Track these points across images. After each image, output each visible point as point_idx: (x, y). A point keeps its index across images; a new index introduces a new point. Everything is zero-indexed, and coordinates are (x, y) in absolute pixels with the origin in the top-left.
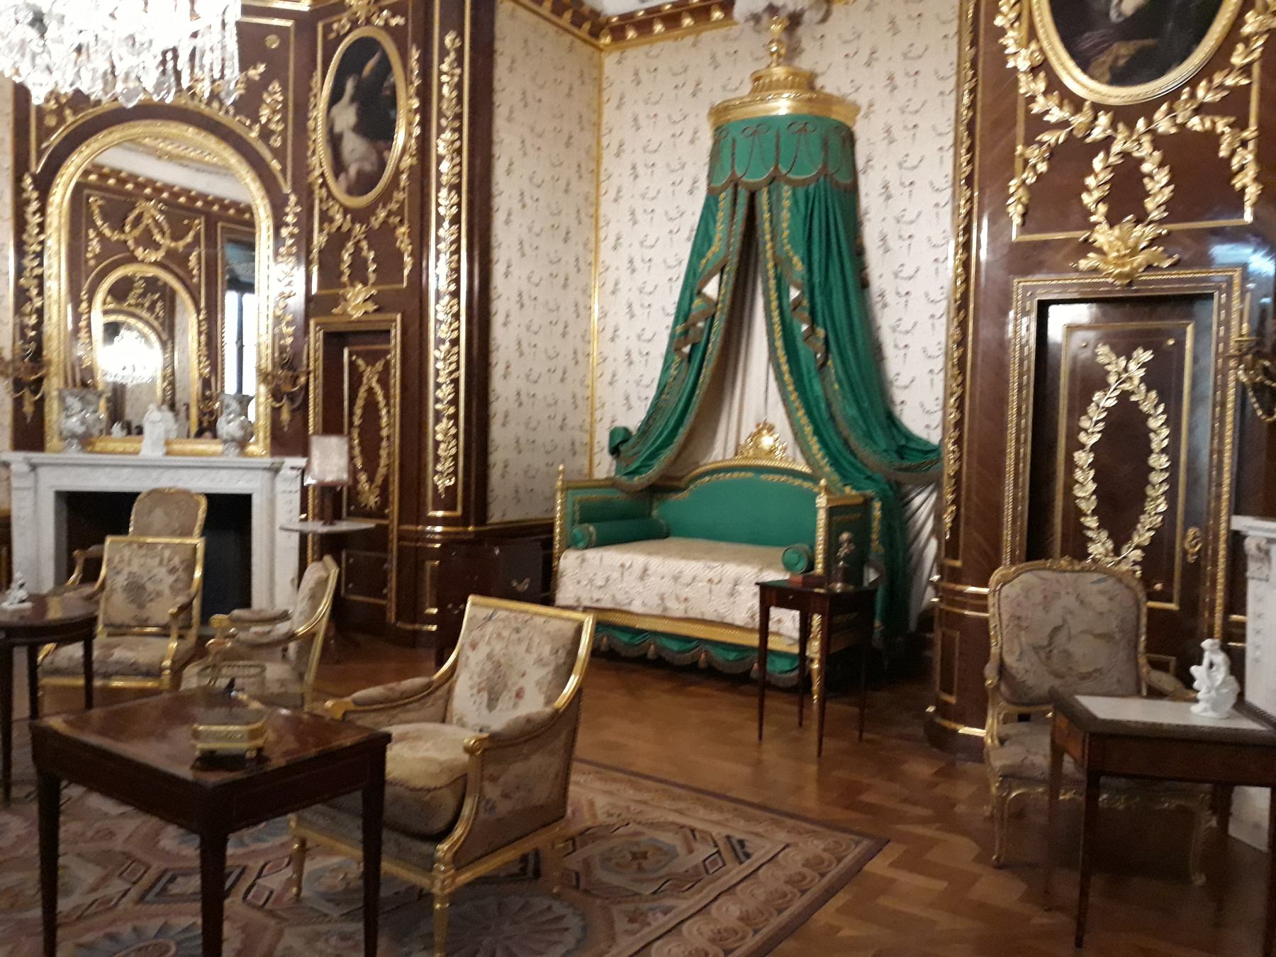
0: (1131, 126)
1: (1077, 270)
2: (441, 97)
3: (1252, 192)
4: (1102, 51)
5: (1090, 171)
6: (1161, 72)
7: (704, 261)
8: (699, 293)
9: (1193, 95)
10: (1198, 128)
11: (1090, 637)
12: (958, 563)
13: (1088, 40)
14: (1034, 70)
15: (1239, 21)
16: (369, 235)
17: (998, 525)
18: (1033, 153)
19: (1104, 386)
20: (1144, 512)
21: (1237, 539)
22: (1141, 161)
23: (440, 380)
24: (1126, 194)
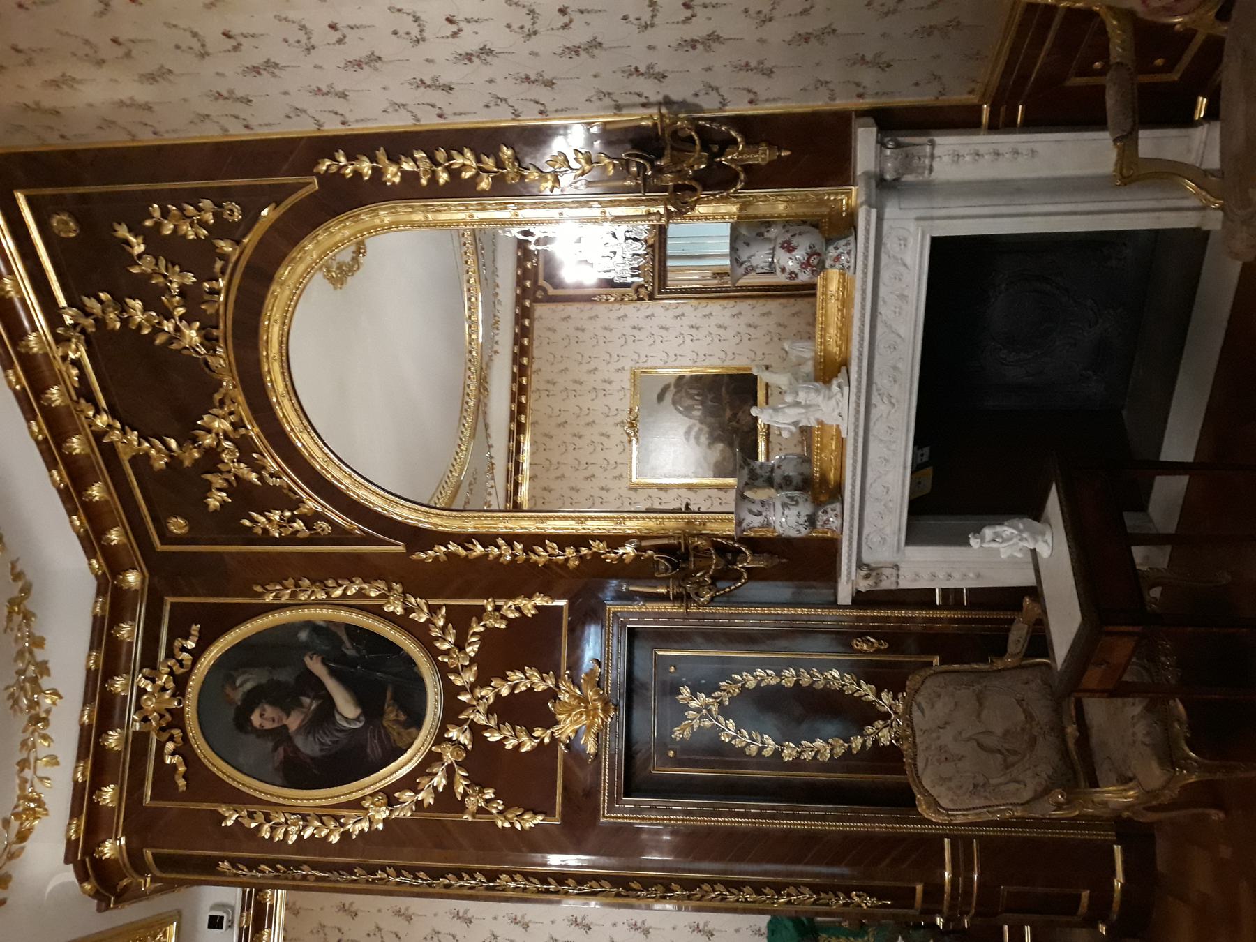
0: (465, 706)
1: (597, 755)
3: (540, 601)
4: (388, 738)
5: (500, 743)
6: (420, 681)
9: (446, 653)
10: (476, 648)
11: (985, 712)
12: (919, 888)
13: (374, 749)
14: (391, 802)
15: (391, 618)
17: (869, 838)
18: (472, 803)
19: (716, 730)
20: (842, 691)
21: (861, 599)
22: (498, 695)
24: (529, 711)
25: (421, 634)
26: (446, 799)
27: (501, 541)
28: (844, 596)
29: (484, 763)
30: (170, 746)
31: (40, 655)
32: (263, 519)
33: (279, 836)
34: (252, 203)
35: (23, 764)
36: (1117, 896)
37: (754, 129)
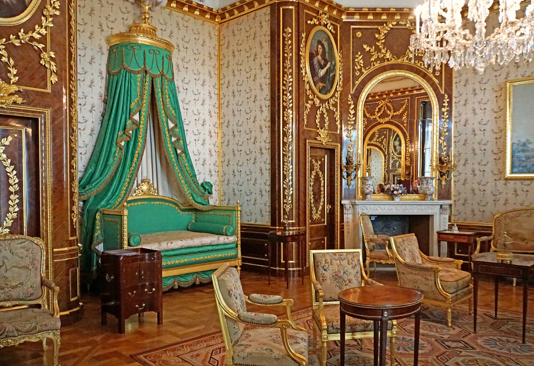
1: (316, 139)
7: (133, 104)
13: (316, 79)
15: (336, 88)
21: (342, 206)
25: (334, 95)
26: (308, 99)
27: (354, 118)
29: (314, 108)
30: (316, 20)
32: (360, 58)
33: (301, 49)
37: (449, 182)
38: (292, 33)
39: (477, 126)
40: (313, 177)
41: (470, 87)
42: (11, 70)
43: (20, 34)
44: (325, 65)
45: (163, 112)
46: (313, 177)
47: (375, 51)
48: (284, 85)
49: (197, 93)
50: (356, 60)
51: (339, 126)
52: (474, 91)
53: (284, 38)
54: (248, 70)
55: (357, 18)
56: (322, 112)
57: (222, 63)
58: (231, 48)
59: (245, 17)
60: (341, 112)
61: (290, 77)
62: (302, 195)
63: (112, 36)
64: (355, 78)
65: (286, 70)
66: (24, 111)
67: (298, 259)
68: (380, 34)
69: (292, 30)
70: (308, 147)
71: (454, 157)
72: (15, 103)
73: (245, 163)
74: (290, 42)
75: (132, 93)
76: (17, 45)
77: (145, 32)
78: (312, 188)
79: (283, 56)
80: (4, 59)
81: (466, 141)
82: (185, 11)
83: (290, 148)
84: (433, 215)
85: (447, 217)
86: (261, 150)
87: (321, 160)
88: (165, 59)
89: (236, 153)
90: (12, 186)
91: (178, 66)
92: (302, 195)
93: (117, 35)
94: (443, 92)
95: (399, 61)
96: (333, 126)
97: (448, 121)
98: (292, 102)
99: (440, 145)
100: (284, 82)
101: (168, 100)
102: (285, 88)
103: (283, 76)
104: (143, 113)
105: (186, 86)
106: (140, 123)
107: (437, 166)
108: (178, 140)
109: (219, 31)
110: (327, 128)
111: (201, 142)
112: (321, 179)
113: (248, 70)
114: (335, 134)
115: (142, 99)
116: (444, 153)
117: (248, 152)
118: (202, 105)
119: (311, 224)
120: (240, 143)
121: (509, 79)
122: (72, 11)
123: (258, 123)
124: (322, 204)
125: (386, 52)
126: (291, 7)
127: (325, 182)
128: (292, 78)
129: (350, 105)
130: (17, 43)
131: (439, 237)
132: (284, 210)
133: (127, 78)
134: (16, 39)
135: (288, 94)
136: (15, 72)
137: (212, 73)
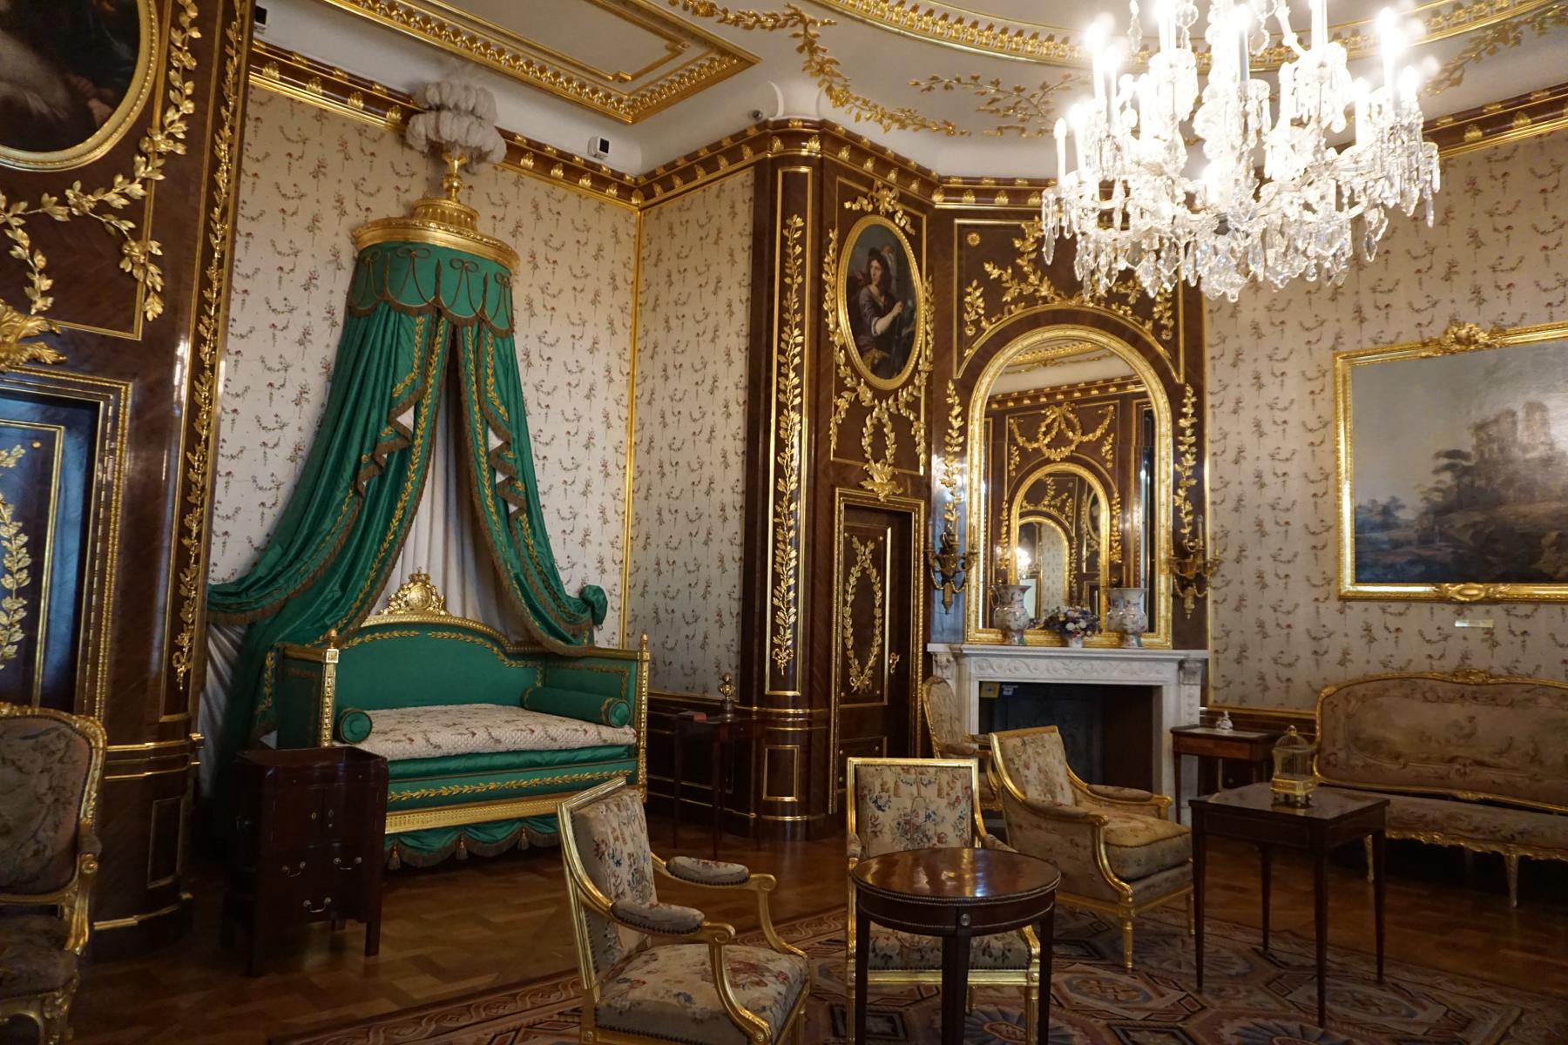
1: (862, 487)
2: (223, 74)
7: (400, 387)
8: (391, 421)
13: (864, 340)
15: (917, 363)
16: (38, 226)
21: (928, 657)
23: (192, 499)
25: (910, 381)
27: (961, 439)
28: (931, 648)
29: (858, 411)
31: (910, 129)
33: (826, 267)
34: (1171, 346)
35: (865, 102)
36: (780, 818)
37: (1201, 603)
38: (803, 229)
39: (1266, 466)
40: (852, 581)
41: (1247, 368)
42: (36, 278)
43: (69, 193)
44: (890, 310)
45: (476, 408)
46: (852, 581)
47: (1013, 278)
48: (781, 352)
49: (574, 369)
50: (968, 299)
51: (922, 457)
52: (1257, 377)
53: (784, 239)
54: (700, 317)
55: (968, 202)
56: (879, 420)
57: (641, 299)
58: (663, 267)
59: (699, 192)
60: (928, 423)
61: (796, 332)
62: (819, 625)
63: (367, 225)
64: (965, 342)
65: (787, 316)
66: (58, 382)
67: (805, 791)
68: (1024, 239)
69: (805, 221)
70: (839, 505)
71: (1213, 539)
72: (35, 360)
73: (686, 544)
74: (798, 249)
75: (400, 362)
76: (59, 218)
77: (444, 219)
78: (848, 609)
79: (782, 283)
80: (18, 252)
81: (1240, 500)
82: (556, 178)
83: (793, 507)
84: (1159, 688)
85: (1197, 691)
86: (723, 510)
87: (875, 540)
88: (491, 284)
89: (666, 516)
90: (12, 574)
91: (530, 304)
92: (819, 625)
93: (376, 224)
94: (1180, 380)
95: (1074, 303)
96: (907, 457)
97: (1194, 450)
98: (801, 395)
99: (1177, 510)
100: (783, 345)
101: (491, 380)
102: (783, 360)
103: (781, 331)
104: (425, 411)
105: (547, 352)
106: (414, 435)
107: (1169, 561)
108: (511, 480)
109: (641, 225)
110: (890, 460)
111: (580, 487)
112: (877, 587)
113: (700, 317)
114: (912, 477)
115: (425, 375)
116: (1186, 531)
117: (693, 516)
118: (588, 397)
119: (843, 701)
120: (676, 493)
121: (1342, 349)
122: (223, 147)
123: (717, 445)
124: (876, 650)
125: (1041, 281)
126: (804, 169)
127: (885, 594)
128: (802, 334)
129: (952, 407)
130: (60, 214)
131: (1176, 744)
132: (773, 662)
133: (391, 325)
134: (57, 204)
135: (792, 375)
136: (46, 284)
137: (618, 324)
